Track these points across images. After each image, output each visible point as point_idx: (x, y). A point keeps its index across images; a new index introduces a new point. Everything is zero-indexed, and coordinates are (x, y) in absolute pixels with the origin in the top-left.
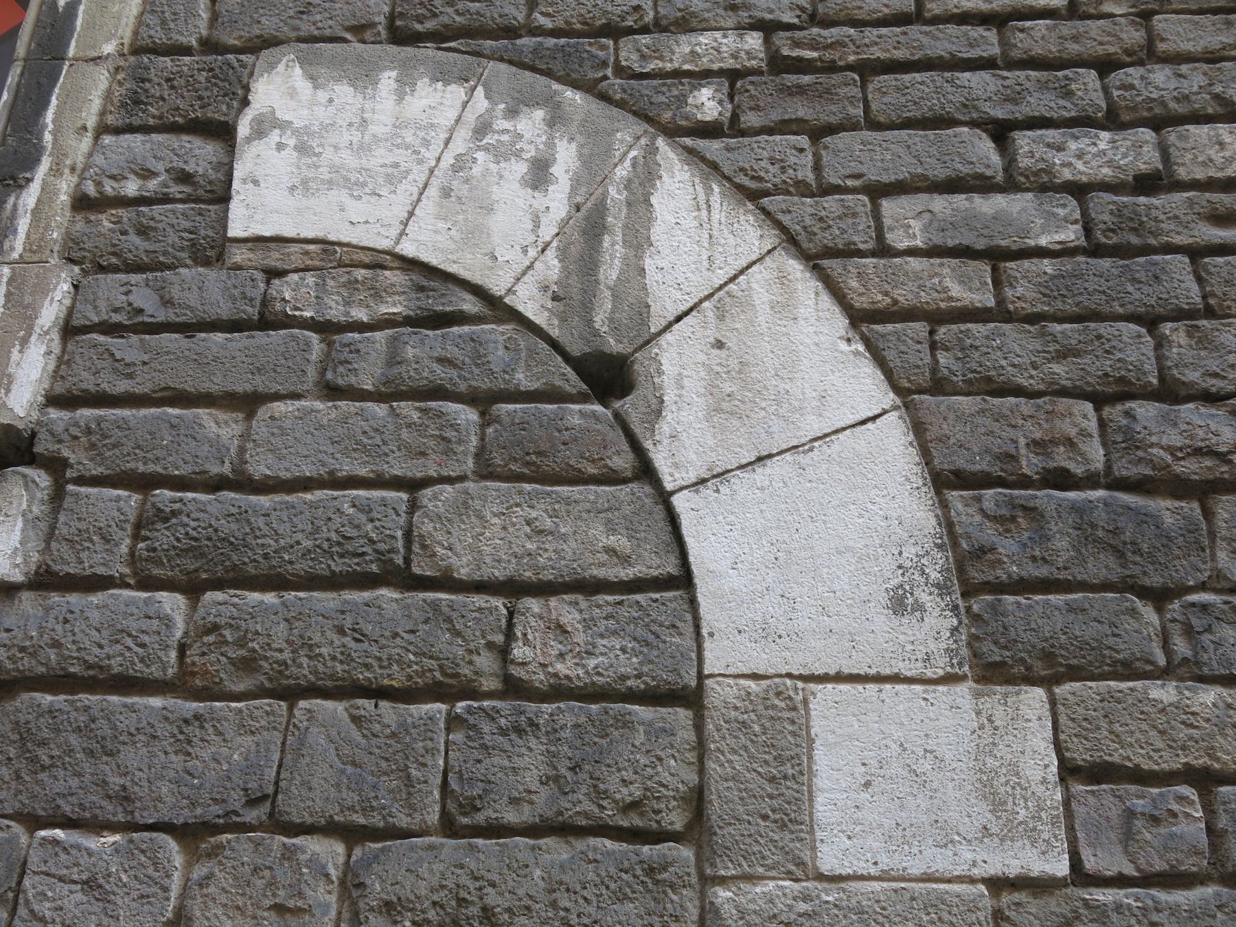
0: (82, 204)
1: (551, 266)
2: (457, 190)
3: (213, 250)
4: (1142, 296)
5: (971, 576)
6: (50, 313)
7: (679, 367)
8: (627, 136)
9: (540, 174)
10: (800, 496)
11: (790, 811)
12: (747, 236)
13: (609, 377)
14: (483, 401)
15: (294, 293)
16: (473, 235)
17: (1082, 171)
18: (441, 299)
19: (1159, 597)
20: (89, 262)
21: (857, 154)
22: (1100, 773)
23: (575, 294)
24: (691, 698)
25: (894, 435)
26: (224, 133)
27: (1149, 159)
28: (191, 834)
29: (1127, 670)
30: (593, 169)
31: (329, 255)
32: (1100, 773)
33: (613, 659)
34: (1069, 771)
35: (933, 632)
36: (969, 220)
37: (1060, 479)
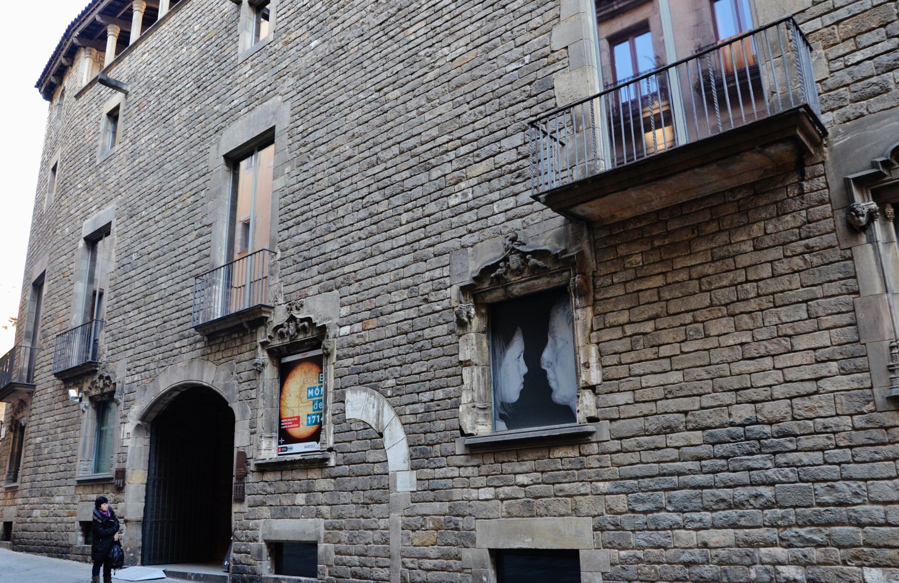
0: (333, 415)
1: (375, 421)
2: (366, 411)
3: (345, 421)
4: (429, 419)
5: (412, 458)
6: (332, 432)
7: (386, 434)
8: (382, 397)
9: (373, 407)
10: (397, 451)
11: (395, 487)
12: (393, 414)
13: (381, 435)
14: (370, 439)
15: (353, 426)
16: (368, 417)
17: (425, 400)
18: (367, 426)
19: (427, 459)
20: (335, 423)
21: (406, 399)
22: (420, 480)
23: (377, 425)
24: (387, 474)
25: (405, 441)
26: (343, 402)
27: (432, 397)
28: (351, 491)
29: (423, 468)
30: (379, 403)
31: (356, 421)
32: (420, 480)
33: (381, 471)
34: (418, 480)
35: (406, 466)
36: (414, 409)
37: (419, 445)
